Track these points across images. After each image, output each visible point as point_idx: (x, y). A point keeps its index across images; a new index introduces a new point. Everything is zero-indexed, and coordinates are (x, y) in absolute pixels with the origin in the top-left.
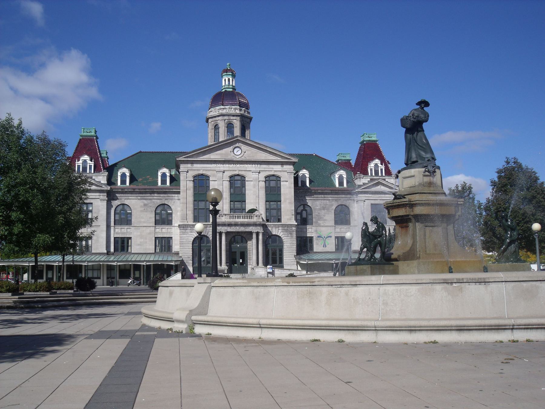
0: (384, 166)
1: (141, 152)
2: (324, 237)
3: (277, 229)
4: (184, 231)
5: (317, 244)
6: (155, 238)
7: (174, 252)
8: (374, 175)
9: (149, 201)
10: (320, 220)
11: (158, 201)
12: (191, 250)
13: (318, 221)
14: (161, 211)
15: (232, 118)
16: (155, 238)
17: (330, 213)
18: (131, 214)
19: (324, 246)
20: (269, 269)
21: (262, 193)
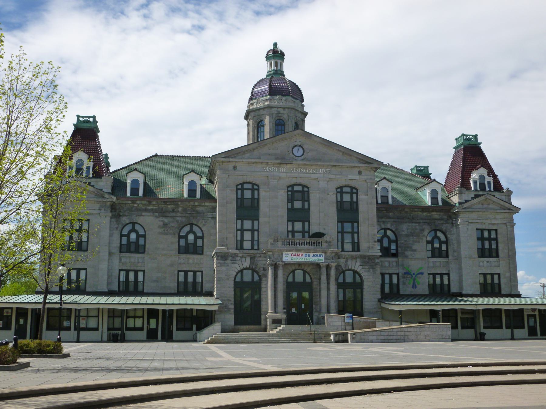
0: (491, 177)
1: (156, 155)
2: (414, 274)
3: (354, 261)
4: (223, 261)
5: (404, 284)
6: (179, 271)
7: (205, 292)
8: (479, 189)
9: (170, 220)
10: (407, 251)
11: (184, 219)
12: (233, 289)
13: (405, 252)
14: (188, 233)
16: (179, 271)
17: (421, 240)
18: (144, 236)
19: (413, 287)
20: (348, 319)
21: (333, 211)
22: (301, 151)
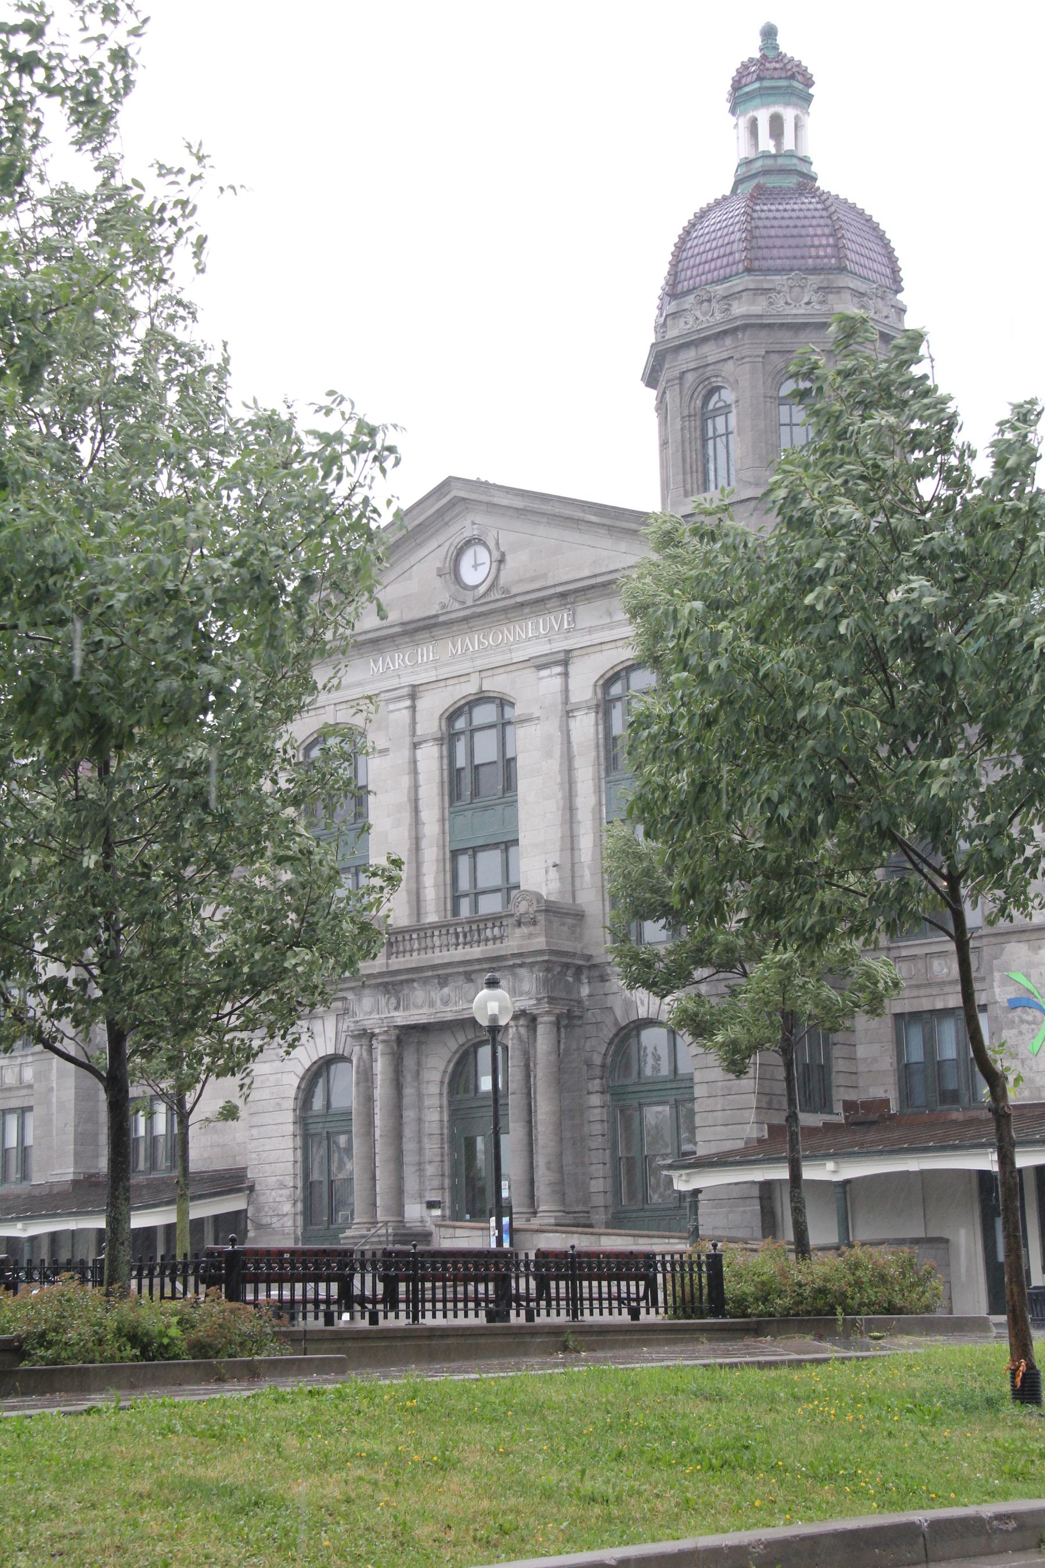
15: (711, 352)
22: (483, 555)
